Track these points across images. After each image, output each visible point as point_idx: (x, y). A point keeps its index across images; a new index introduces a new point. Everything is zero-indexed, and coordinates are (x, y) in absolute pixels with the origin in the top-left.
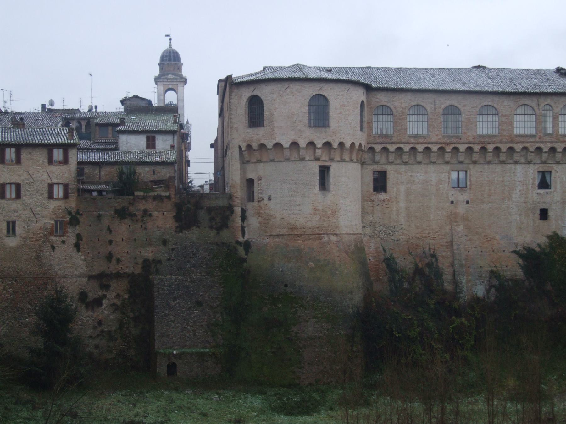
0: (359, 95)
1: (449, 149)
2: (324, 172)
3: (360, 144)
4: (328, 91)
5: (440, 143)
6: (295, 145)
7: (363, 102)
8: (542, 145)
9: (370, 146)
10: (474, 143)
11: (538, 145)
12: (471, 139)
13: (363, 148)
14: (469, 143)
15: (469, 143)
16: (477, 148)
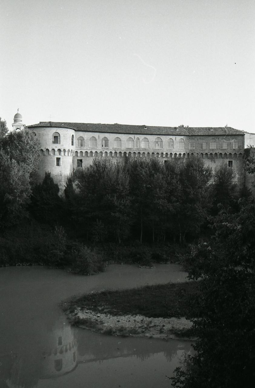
0: (71, 132)
1: (104, 152)
2: (58, 159)
3: (72, 150)
4: (60, 131)
5: (101, 150)
6: (48, 150)
7: (73, 135)
8: (136, 152)
9: (76, 150)
10: (112, 150)
11: (134, 151)
12: (111, 149)
13: (73, 151)
14: (111, 150)
15: (111, 150)
16: (113, 152)
